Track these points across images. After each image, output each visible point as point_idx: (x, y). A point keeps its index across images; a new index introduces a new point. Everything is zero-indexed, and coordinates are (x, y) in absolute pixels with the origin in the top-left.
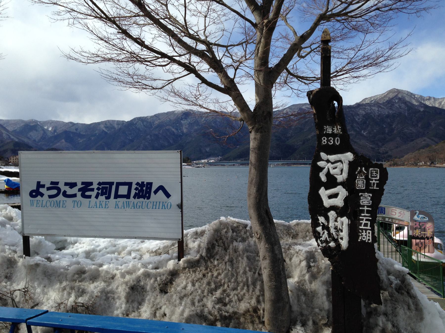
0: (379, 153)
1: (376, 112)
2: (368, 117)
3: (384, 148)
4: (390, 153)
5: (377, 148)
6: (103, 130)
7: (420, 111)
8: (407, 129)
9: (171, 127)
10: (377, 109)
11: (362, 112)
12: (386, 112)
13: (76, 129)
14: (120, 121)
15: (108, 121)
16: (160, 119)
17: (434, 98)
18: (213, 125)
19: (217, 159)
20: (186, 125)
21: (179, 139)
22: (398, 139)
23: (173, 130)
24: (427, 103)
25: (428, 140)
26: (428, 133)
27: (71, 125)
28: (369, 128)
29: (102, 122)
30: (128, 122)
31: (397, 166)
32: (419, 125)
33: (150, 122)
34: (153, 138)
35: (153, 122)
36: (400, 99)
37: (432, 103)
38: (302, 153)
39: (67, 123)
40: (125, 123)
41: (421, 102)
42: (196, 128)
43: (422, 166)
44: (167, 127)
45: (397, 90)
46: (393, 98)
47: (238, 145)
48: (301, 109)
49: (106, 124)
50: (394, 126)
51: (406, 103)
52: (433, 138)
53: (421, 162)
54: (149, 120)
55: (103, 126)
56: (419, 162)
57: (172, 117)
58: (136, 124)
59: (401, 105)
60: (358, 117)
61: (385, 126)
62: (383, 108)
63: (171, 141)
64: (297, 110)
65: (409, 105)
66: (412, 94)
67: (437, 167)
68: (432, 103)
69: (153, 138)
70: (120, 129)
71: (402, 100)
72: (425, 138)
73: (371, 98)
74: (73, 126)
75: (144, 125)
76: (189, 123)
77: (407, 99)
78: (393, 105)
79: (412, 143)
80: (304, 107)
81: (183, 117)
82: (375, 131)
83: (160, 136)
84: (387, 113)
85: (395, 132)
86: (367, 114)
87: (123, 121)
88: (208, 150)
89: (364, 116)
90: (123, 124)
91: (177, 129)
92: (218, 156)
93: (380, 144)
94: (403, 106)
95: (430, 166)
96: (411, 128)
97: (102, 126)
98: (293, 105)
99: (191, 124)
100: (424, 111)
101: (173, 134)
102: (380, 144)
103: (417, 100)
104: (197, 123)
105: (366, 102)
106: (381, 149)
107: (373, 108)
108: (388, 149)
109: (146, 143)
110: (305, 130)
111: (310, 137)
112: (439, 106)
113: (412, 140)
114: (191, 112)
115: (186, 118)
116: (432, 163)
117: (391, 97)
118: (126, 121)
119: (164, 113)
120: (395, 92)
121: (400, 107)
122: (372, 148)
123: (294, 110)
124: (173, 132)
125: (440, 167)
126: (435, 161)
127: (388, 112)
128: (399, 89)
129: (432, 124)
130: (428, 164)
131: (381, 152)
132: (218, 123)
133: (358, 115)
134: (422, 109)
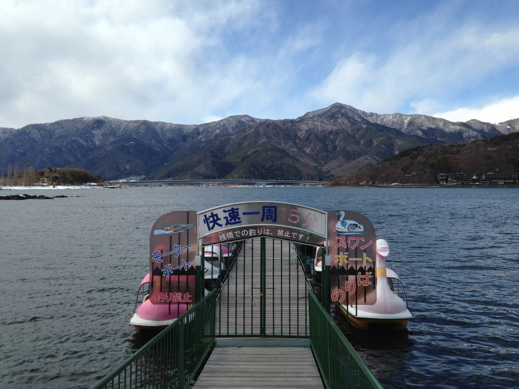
0: (322, 172)
1: (319, 127)
3: (326, 167)
4: (333, 172)
7: (362, 128)
8: (350, 147)
9: (78, 138)
10: (320, 124)
11: (304, 127)
17: (376, 114)
18: (135, 137)
19: (139, 178)
21: (90, 153)
22: (341, 157)
23: (82, 141)
24: (370, 119)
25: (370, 158)
28: (312, 145)
32: (362, 143)
33: (50, 131)
34: (53, 151)
35: (53, 131)
36: (343, 115)
37: (375, 119)
38: (240, 172)
40: (13, 131)
41: (364, 119)
42: (112, 139)
44: (73, 139)
45: (340, 104)
46: (336, 113)
47: (165, 162)
48: (239, 121)
50: (337, 143)
54: (48, 129)
57: (80, 126)
58: (29, 133)
59: (344, 121)
64: (235, 123)
65: (352, 121)
66: (355, 109)
68: (375, 119)
69: (53, 151)
70: (7, 139)
71: (345, 115)
72: (367, 157)
73: (314, 112)
76: (103, 133)
77: (350, 114)
78: (336, 120)
79: (354, 161)
80: (242, 120)
81: (94, 126)
82: (318, 148)
83: (63, 149)
84: (330, 129)
85: (338, 149)
86: (310, 129)
88: (128, 167)
89: (307, 132)
90: (12, 132)
91: (87, 141)
92: (141, 175)
93: (323, 162)
94: (346, 122)
98: (231, 117)
99: (106, 134)
100: (366, 128)
101: (82, 146)
102: (323, 162)
103: (360, 117)
104: (113, 132)
105: (309, 116)
106: (324, 168)
107: (316, 123)
109: (44, 158)
110: (244, 146)
111: (249, 153)
112: (381, 123)
113: (355, 159)
114: (106, 121)
115: (98, 127)
117: (334, 112)
119: (69, 120)
120: (338, 107)
121: (343, 123)
122: (315, 167)
124: (82, 144)
127: (331, 128)
128: (342, 103)
129: (374, 141)
131: (324, 171)
132: (140, 134)
133: (301, 130)
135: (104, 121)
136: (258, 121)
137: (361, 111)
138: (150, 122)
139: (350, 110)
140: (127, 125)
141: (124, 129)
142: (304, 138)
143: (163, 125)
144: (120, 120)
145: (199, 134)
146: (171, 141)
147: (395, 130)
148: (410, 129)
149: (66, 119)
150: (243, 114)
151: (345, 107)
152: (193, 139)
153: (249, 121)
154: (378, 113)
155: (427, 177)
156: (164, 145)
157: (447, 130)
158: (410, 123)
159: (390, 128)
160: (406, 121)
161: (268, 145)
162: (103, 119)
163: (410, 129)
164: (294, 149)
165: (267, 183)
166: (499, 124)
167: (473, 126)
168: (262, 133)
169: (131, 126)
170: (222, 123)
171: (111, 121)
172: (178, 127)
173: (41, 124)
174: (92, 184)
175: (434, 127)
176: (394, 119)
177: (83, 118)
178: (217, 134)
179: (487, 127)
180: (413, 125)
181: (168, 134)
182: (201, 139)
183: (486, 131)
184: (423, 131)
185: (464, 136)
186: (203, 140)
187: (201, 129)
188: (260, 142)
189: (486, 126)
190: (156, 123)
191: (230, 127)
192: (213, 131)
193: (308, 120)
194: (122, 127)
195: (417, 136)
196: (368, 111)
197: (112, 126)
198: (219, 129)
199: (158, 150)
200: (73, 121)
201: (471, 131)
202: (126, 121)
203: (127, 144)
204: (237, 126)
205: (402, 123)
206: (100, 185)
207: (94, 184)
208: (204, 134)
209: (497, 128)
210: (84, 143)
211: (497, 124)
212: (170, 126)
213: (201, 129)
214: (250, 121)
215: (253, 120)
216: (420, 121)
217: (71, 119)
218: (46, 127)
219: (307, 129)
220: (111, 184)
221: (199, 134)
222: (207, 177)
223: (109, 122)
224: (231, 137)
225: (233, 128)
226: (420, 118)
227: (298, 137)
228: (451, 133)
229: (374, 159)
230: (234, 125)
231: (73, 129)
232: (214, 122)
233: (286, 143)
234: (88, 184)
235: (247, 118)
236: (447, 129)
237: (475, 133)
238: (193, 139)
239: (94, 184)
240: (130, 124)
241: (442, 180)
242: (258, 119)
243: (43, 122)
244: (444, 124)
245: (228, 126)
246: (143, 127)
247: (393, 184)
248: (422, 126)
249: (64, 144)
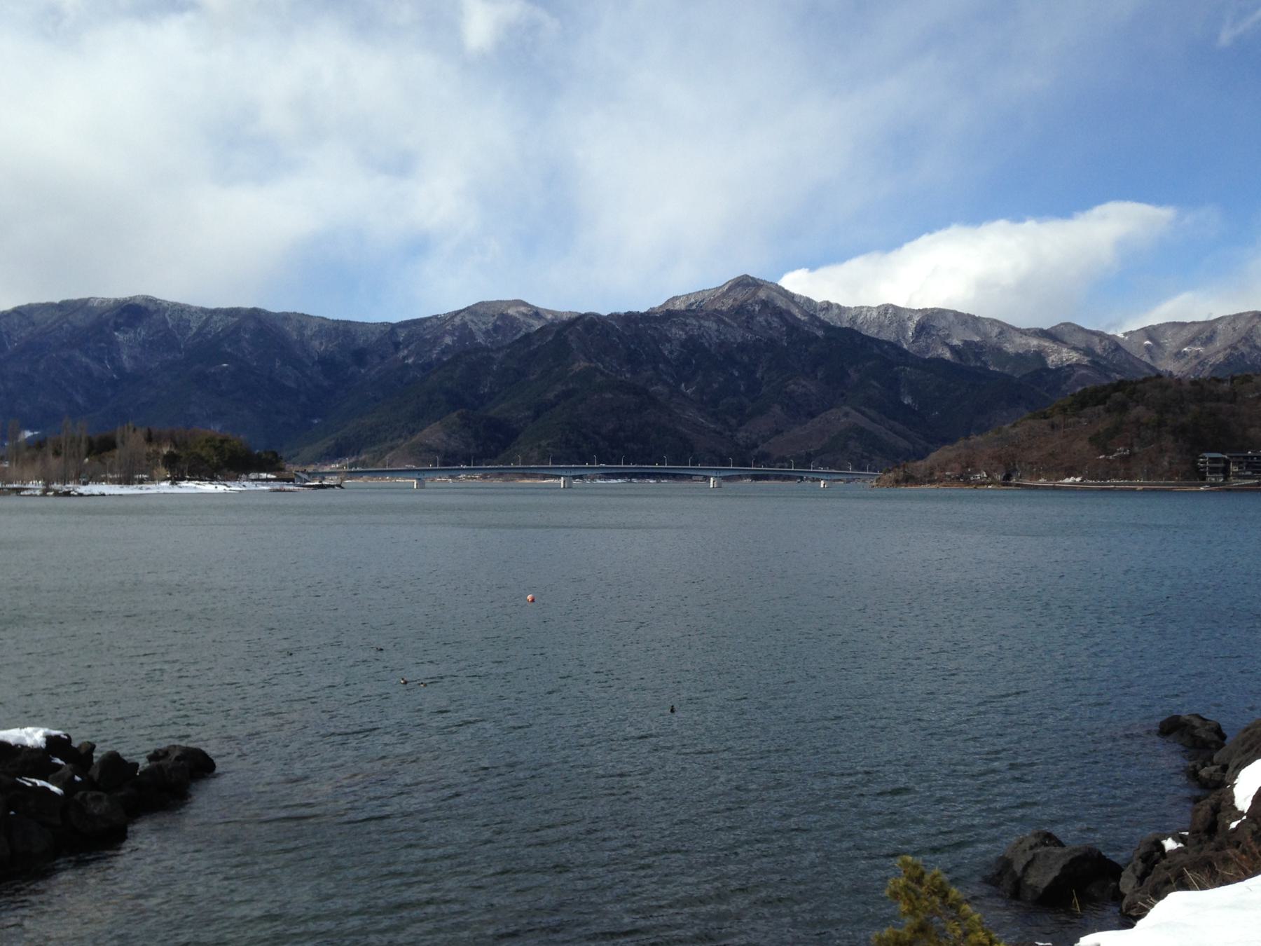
2: (693, 346)
4: (763, 447)
5: (728, 433)
7: (817, 337)
8: (796, 384)
9: (77, 353)
10: (714, 326)
11: (677, 333)
17: (838, 306)
22: (777, 409)
24: (821, 316)
26: (842, 395)
36: (765, 304)
38: (544, 443)
43: (983, 484)
45: (753, 278)
48: (504, 316)
50: (758, 375)
52: (863, 408)
53: (978, 471)
56: (970, 473)
60: (668, 345)
61: (736, 374)
63: (80, 400)
64: (492, 319)
78: (752, 318)
79: (816, 420)
80: (511, 311)
81: (120, 320)
82: (715, 386)
84: (740, 340)
86: (690, 338)
91: (101, 361)
93: (733, 422)
94: (775, 322)
98: (482, 304)
102: (733, 422)
106: (740, 435)
107: (706, 324)
108: (754, 437)
110: (532, 378)
111: (551, 396)
113: (812, 415)
114: (152, 307)
116: (1008, 477)
120: (748, 285)
121: (769, 323)
122: (715, 431)
123: (483, 319)
129: (851, 372)
130: (999, 478)
131: (741, 442)
132: (244, 344)
133: (669, 340)
134: (820, 333)
135: (146, 309)
136: (549, 317)
138: (268, 314)
140: (206, 323)
141: (200, 329)
143: (302, 321)
144: (189, 307)
145: (397, 346)
146: (327, 364)
147: (888, 343)
148: (922, 342)
149: (44, 301)
150: (510, 298)
152: (383, 358)
153: (523, 314)
154: (842, 304)
155: (1170, 463)
156: (308, 372)
157: (1009, 348)
160: (912, 325)
161: (599, 379)
162: (143, 304)
163: (922, 342)
164: (659, 387)
165: (722, 474)
166: (1125, 334)
167: (1066, 338)
168: (574, 345)
169: (219, 325)
170: (457, 320)
171: (166, 309)
172: (341, 328)
174: (264, 475)
175: (977, 339)
177: (89, 299)
178: (447, 345)
179: (1101, 341)
182: (405, 358)
183: (1099, 350)
184: (953, 349)
185: (1049, 362)
186: (410, 361)
187: (402, 335)
189: (1096, 340)
190: (286, 317)
191: (480, 330)
192: (437, 339)
193: (684, 316)
194: (194, 326)
195: (940, 361)
197: (165, 322)
198: (452, 334)
199: (293, 385)
200: (64, 306)
201: (1065, 350)
202: (203, 310)
204: (496, 328)
205: (902, 327)
206: (288, 480)
207: (269, 476)
208: (412, 347)
209: (1122, 345)
210: (94, 366)
211: (1120, 335)
212: (320, 325)
213: (402, 335)
215: (537, 314)
216: (943, 323)
217: (57, 301)
219: (684, 337)
220: (313, 475)
221: (397, 346)
222: (450, 461)
223: (157, 311)
225: (487, 332)
226: (945, 318)
228: (1018, 355)
229: (863, 413)
230: (490, 326)
231: (61, 327)
232: (436, 317)
234: (252, 476)
235: (523, 309)
236: (1007, 345)
237: (1074, 357)
238: (383, 358)
239: (269, 476)
240: (215, 318)
241: (1214, 471)
242: (548, 311)
244: (1001, 333)
245: (474, 328)
246: (251, 325)
247: (1067, 480)
249: (42, 367)
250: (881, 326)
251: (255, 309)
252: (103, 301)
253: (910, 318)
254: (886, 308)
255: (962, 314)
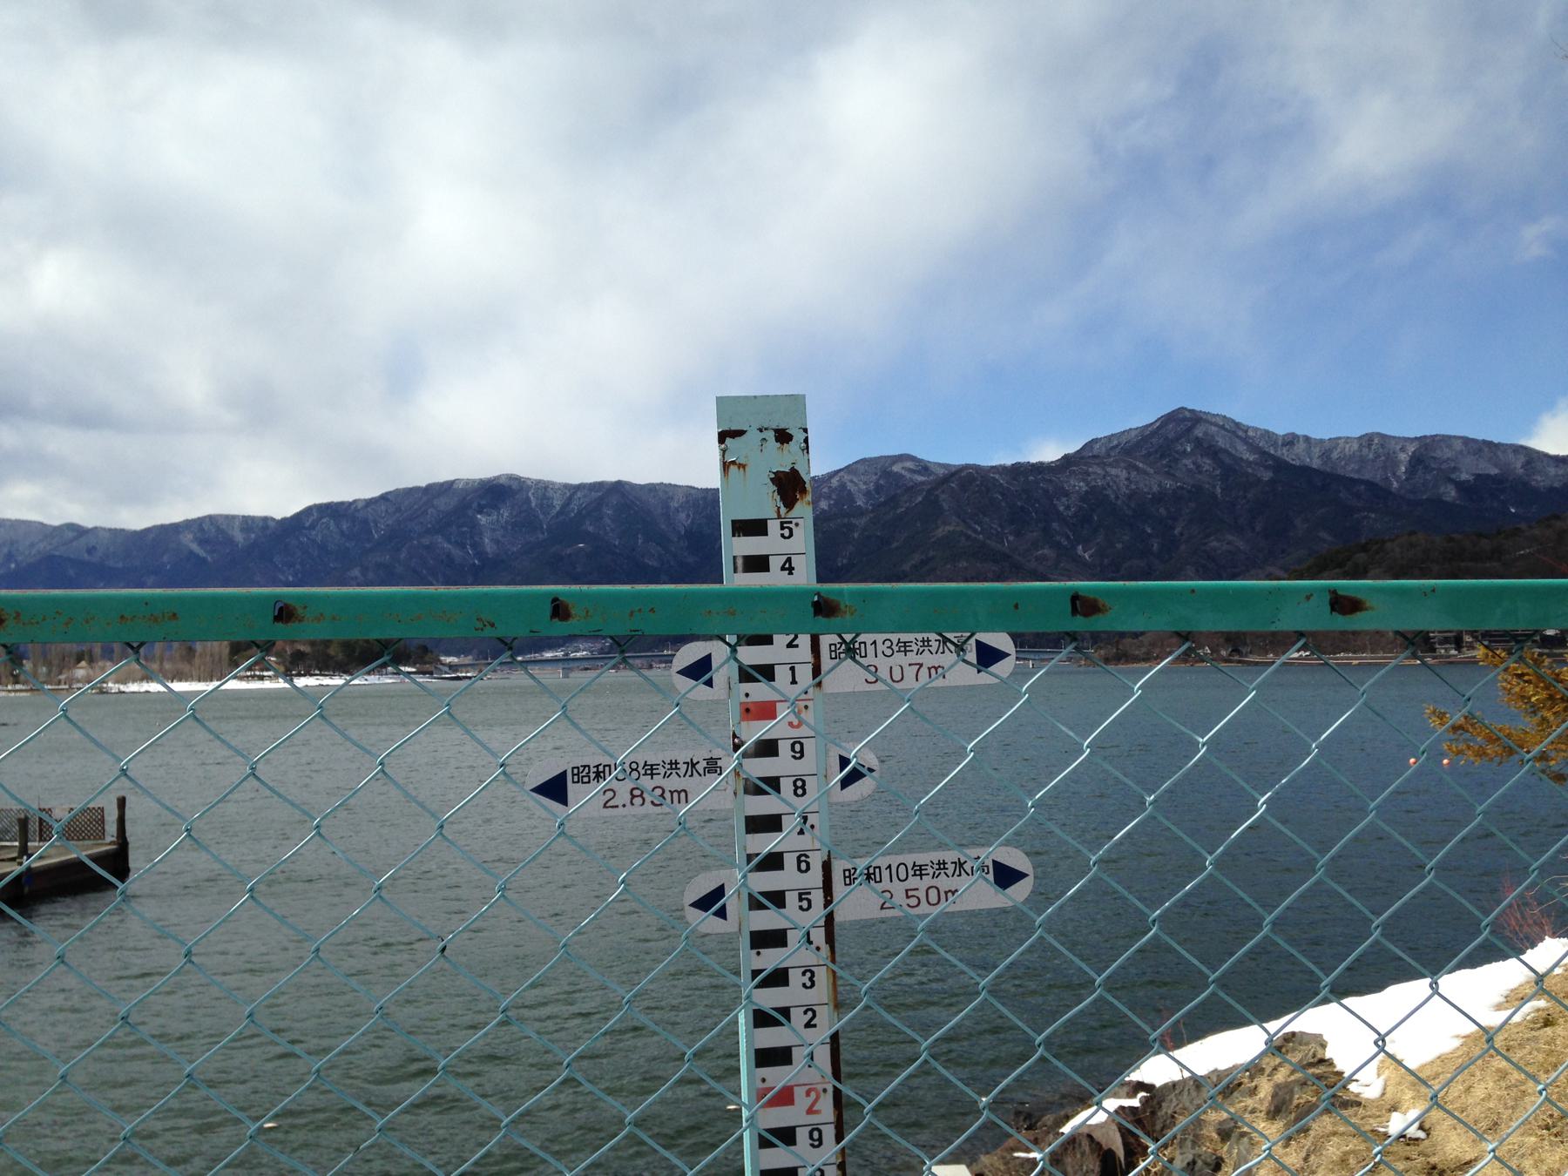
6: (191, 552)
9: (439, 539)
12: (1153, 482)
13: (91, 550)
14: (253, 519)
15: (210, 517)
16: (398, 510)
17: (1307, 439)
18: (591, 529)
20: (494, 530)
24: (1285, 454)
27: (71, 534)
29: (188, 525)
30: (284, 520)
31: (1127, 662)
33: (365, 521)
39: (55, 528)
40: (271, 524)
44: (426, 541)
49: (201, 529)
51: (1216, 453)
55: (190, 536)
57: (444, 504)
58: (312, 527)
62: (1145, 473)
65: (1227, 460)
66: (1238, 425)
67: (1249, 663)
71: (1208, 449)
73: (1110, 438)
74: (75, 538)
75: (342, 533)
77: (1221, 442)
80: (896, 468)
87: (265, 519)
89: (1084, 498)
91: (463, 546)
95: (1226, 661)
96: (1230, 538)
97: (187, 539)
98: (863, 461)
100: (1272, 482)
105: (1095, 452)
112: (1325, 463)
114: (515, 486)
118: (278, 517)
120: (1185, 419)
124: (449, 555)
125: (1257, 664)
126: (1245, 644)
137: (1256, 429)
138: (633, 486)
139: (1222, 427)
140: (570, 499)
142: (1075, 515)
144: (553, 483)
147: (1371, 485)
151: (1207, 421)
153: (910, 470)
157: (1539, 481)
158: (1417, 462)
159: (1352, 480)
160: (1403, 457)
170: (835, 482)
171: (529, 488)
173: (342, 503)
175: (1494, 471)
176: (1365, 451)
177: (453, 482)
180: (1426, 467)
181: (682, 516)
184: (1460, 486)
188: (941, 532)
190: (652, 488)
191: (860, 491)
194: (558, 503)
195: (1438, 502)
196: (1280, 429)
198: (829, 498)
199: (655, 564)
202: (566, 486)
203: (569, 551)
204: (878, 488)
205: (1390, 461)
210: (457, 553)
214: (918, 472)
215: (924, 467)
216: (1448, 454)
218: (357, 510)
223: (521, 489)
224: (854, 521)
225: (868, 494)
226: (1449, 446)
227: (1058, 512)
233: (1018, 534)
235: (909, 464)
242: (940, 465)
243: (347, 496)
246: (614, 500)
248: (1455, 469)
250: (1363, 461)
251: (619, 483)
252: (468, 482)
253: (1403, 449)
254: (1368, 440)
255: (1474, 441)
